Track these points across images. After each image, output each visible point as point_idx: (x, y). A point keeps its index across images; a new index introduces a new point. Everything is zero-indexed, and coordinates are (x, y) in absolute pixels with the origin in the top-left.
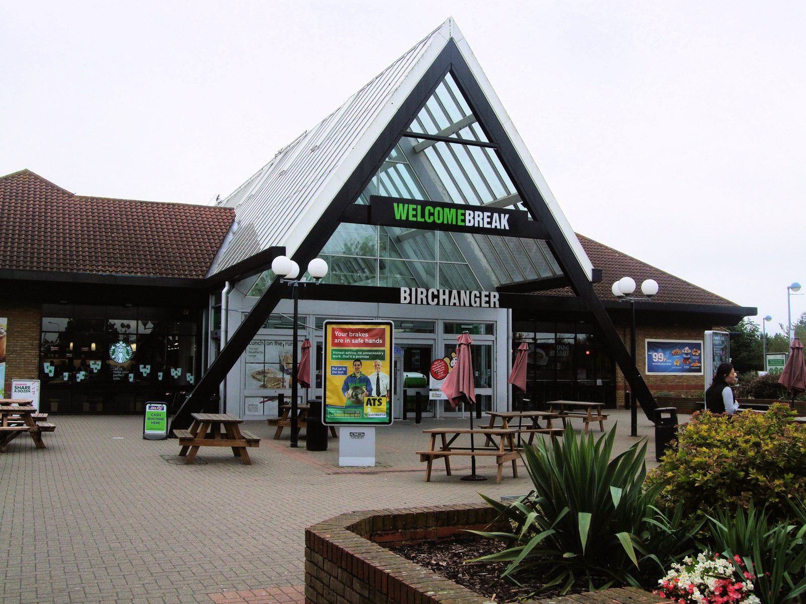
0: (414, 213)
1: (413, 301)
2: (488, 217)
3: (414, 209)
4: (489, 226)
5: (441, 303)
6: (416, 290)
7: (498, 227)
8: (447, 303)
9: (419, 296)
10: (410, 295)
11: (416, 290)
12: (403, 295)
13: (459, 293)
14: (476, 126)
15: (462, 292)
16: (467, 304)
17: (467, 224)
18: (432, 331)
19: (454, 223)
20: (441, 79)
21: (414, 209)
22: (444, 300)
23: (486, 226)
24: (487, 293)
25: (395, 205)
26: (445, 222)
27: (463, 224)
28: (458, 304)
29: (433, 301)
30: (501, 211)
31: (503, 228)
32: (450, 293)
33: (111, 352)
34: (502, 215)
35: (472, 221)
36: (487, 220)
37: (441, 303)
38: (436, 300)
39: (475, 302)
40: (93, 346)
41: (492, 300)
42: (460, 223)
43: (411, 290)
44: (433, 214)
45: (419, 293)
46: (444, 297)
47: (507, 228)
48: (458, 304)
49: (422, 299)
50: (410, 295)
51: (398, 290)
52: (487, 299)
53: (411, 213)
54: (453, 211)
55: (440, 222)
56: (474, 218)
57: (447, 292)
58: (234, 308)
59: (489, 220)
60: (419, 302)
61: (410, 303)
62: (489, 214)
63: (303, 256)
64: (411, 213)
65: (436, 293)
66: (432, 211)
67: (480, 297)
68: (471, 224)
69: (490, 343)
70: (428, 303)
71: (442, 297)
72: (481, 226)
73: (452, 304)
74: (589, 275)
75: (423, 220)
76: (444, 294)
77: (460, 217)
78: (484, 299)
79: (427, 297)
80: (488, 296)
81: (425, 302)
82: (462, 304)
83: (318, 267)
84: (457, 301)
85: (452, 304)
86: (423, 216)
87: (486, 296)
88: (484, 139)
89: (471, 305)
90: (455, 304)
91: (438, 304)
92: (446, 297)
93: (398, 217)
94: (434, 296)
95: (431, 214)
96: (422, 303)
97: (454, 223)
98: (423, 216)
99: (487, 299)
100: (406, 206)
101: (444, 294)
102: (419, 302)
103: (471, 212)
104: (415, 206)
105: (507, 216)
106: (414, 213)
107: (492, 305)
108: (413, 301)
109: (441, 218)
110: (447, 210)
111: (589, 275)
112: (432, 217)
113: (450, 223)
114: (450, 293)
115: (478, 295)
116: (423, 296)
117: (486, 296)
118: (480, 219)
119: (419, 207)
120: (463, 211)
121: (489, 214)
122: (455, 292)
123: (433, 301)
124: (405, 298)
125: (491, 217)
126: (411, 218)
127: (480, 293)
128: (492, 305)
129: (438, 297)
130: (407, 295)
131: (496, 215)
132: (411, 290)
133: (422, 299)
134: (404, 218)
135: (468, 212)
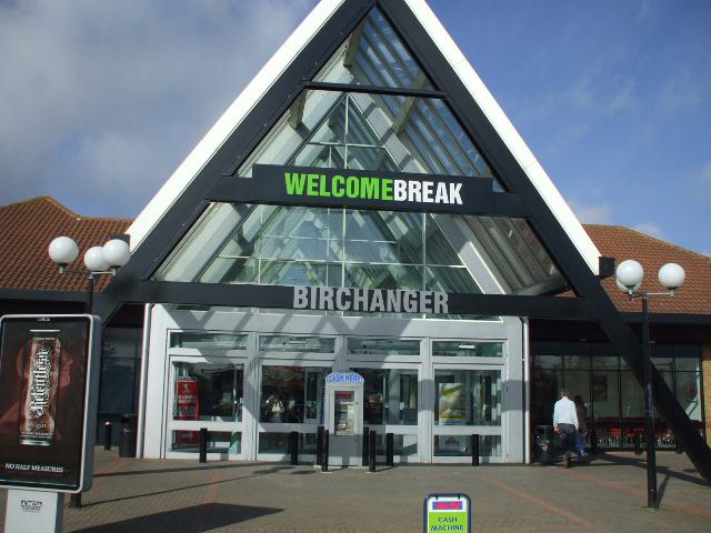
0: (316, 185)
1: (313, 306)
2: (430, 188)
3: (314, 181)
4: (431, 200)
5: (356, 307)
9: (323, 298)
10: (309, 296)
12: (297, 297)
16: (397, 308)
17: (397, 198)
21: (314, 181)
22: (361, 304)
23: (426, 200)
24: (429, 293)
25: (287, 176)
26: (363, 196)
27: (390, 198)
28: (382, 309)
29: (343, 304)
30: (448, 180)
31: (452, 202)
34: (452, 185)
35: (404, 194)
36: (427, 192)
37: (356, 307)
39: (410, 306)
41: (437, 303)
42: (385, 197)
43: (309, 289)
44: (344, 186)
46: (361, 299)
47: (460, 202)
48: (382, 309)
49: (326, 302)
50: (309, 296)
53: (311, 185)
54: (375, 181)
55: (354, 196)
56: (407, 190)
60: (322, 306)
61: (308, 307)
62: (432, 184)
64: (311, 185)
65: (348, 293)
66: (342, 181)
67: (418, 299)
68: (403, 198)
71: (357, 299)
72: (419, 200)
73: (373, 309)
74: (595, 268)
75: (328, 194)
77: (385, 190)
78: (424, 301)
79: (334, 298)
81: (330, 306)
82: (389, 309)
85: (373, 309)
86: (329, 188)
87: (427, 297)
89: (403, 310)
90: (378, 309)
92: (365, 299)
93: (290, 191)
95: (340, 186)
96: (326, 308)
97: (377, 197)
98: (329, 188)
99: (429, 302)
100: (303, 176)
102: (322, 306)
103: (403, 182)
104: (316, 177)
105: (459, 186)
106: (316, 185)
107: (437, 310)
108: (313, 306)
109: (357, 188)
110: (365, 180)
111: (595, 268)
112: (342, 191)
113: (369, 197)
115: (415, 296)
116: (329, 299)
117: (427, 297)
118: (417, 191)
119: (323, 178)
120: (390, 181)
121: (432, 184)
123: (343, 304)
124: (301, 301)
125: (434, 188)
126: (310, 192)
127: (418, 293)
129: (351, 299)
130: (303, 297)
131: (442, 185)
132: (309, 289)
133: (326, 302)
134: (299, 192)
135: (397, 182)
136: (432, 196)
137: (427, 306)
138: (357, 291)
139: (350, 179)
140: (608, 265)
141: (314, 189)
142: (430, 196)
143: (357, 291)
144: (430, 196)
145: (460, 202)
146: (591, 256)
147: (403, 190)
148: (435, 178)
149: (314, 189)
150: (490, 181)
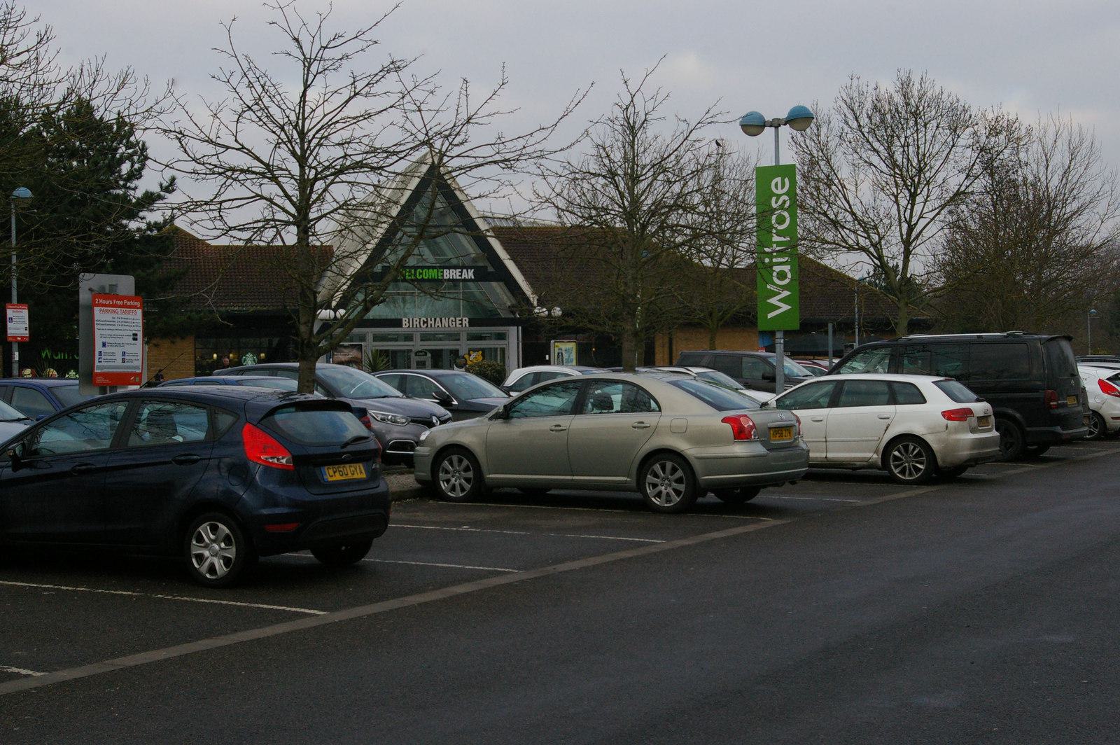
8: (433, 326)
10: (409, 322)
15: (443, 319)
16: (447, 326)
18: (459, 340)
19: (436, 278)
22: (431, 325)
23: (458, 278)
30: (467, 268)
33: (243, 360)
34: (469, 270)
35: (448, 275)
36: (458, 274)
40: (215, 356)
45: (414, 321)
47: (473, 278)
50: (409, 322)
51: (401, 320)
52: (460, 322)
54: (435, 270)
60: (415, 326)
62: (460, 270)
66: (421, 271)
69: (504, 346)
70: (420, 327)
71: (429, 322)
72: (455, 278)
76: (431, 320)
78: (458, 322)
79: (420, 323)
80: (461, 320)
82: (443, 326)
84: (440, 324)
91: (427, 327)
94: (424, 322)
95: (420, 274)
99: (460, 322)
101: (431, 320)
102: (415, 326)
105: (473, 270)
107: (464, 326)
110: (431, 270)
116: (418, 323)
119: (413, 271)
121: (460, 270)
122: (438, 319)
125: (461, 272)
128: (464, 326)
129: (427, 322)
130: (407, 322)
135: (445, 270)
136: (461, 276)
137: (460, 324)
138: (429, 319)
139: (424, 271)
143: (429, 319)
148: (462, 267)
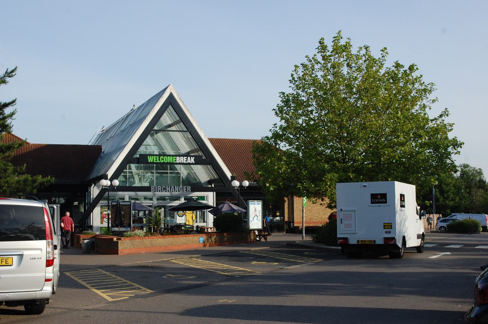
0: (156, 159)
3: (156, 158)
4: (186, 162)
6: (157, 187)
7: (190, 162)
10: (155, 189)
11: (157, 187)
13: (174, 187)
14: (181, 124)
15: (176, 187)
17: (177, 162)
19: (172, 162)
20: (168, 107)
21: (156, 158)
22: (168, 190)
24: (186, 187)
25: (148, 157)
26: (168, 162)
29: (164, 190)
31: (192, 162)
32: (171, 187)
34: (192, 158)
35: (179, 161)
36: (185, 160)
37: (167, 191)
38: (165, 190)
44: (163, 159)
45: (158, 188)
46: (168, 189)
47: (194, 162)
48: (174, 191)
50: (155, 189)
53: (155, 159)
54: (172, 157)
55: (166, 162)
57: (169, 187)
58: (95, 191)
59: (186, 160)
61: (155, 191)
62: (186, 158)
63: (116, 176)
64: (155, 159)
65: (165, 188)
66: (163, 158)
68: (179, 162)
71: (167, 189)
72: (183, 162)
73: (171, 191)
74: (230, 178)
75: (159, 162)
76: (168, 188)
77: (174, 160)
79: (161, 189)
83: (116, 182)
84: (173, 190)
86: (159, 160)
88: (185, 129)
93: (149, 161)
98: (159, 160)
100: (153, 157)
101: (168, 188)
103: (179, 157)
104: (156, 157)
105: (194, 158)
106: (156, 159)
109: (167, 160)
110: (169, 157)
111: (230, 178)
112: (163, 160)
113: (170, 162)
114: (171, 187)
115: (182, 188)
119: (158, 157)
120: (175, 157)
122: (173, 187)
123: (164, 190)
126: (155, 161)
129: (166, 189)
131: (189, 158)
134: (152, 161)
135: (177, 157)
136: (187, 161)
138: (167, 187)
139: (165, 157)
140: (233, 178)
141: (156, 160)
142: (186, 161)
143: (167, 187)
144: (186, 161)
145: (194, 162)
146: (229, 174)
147: (179, 159)
149: (156, 160)
150: (202, 156)
